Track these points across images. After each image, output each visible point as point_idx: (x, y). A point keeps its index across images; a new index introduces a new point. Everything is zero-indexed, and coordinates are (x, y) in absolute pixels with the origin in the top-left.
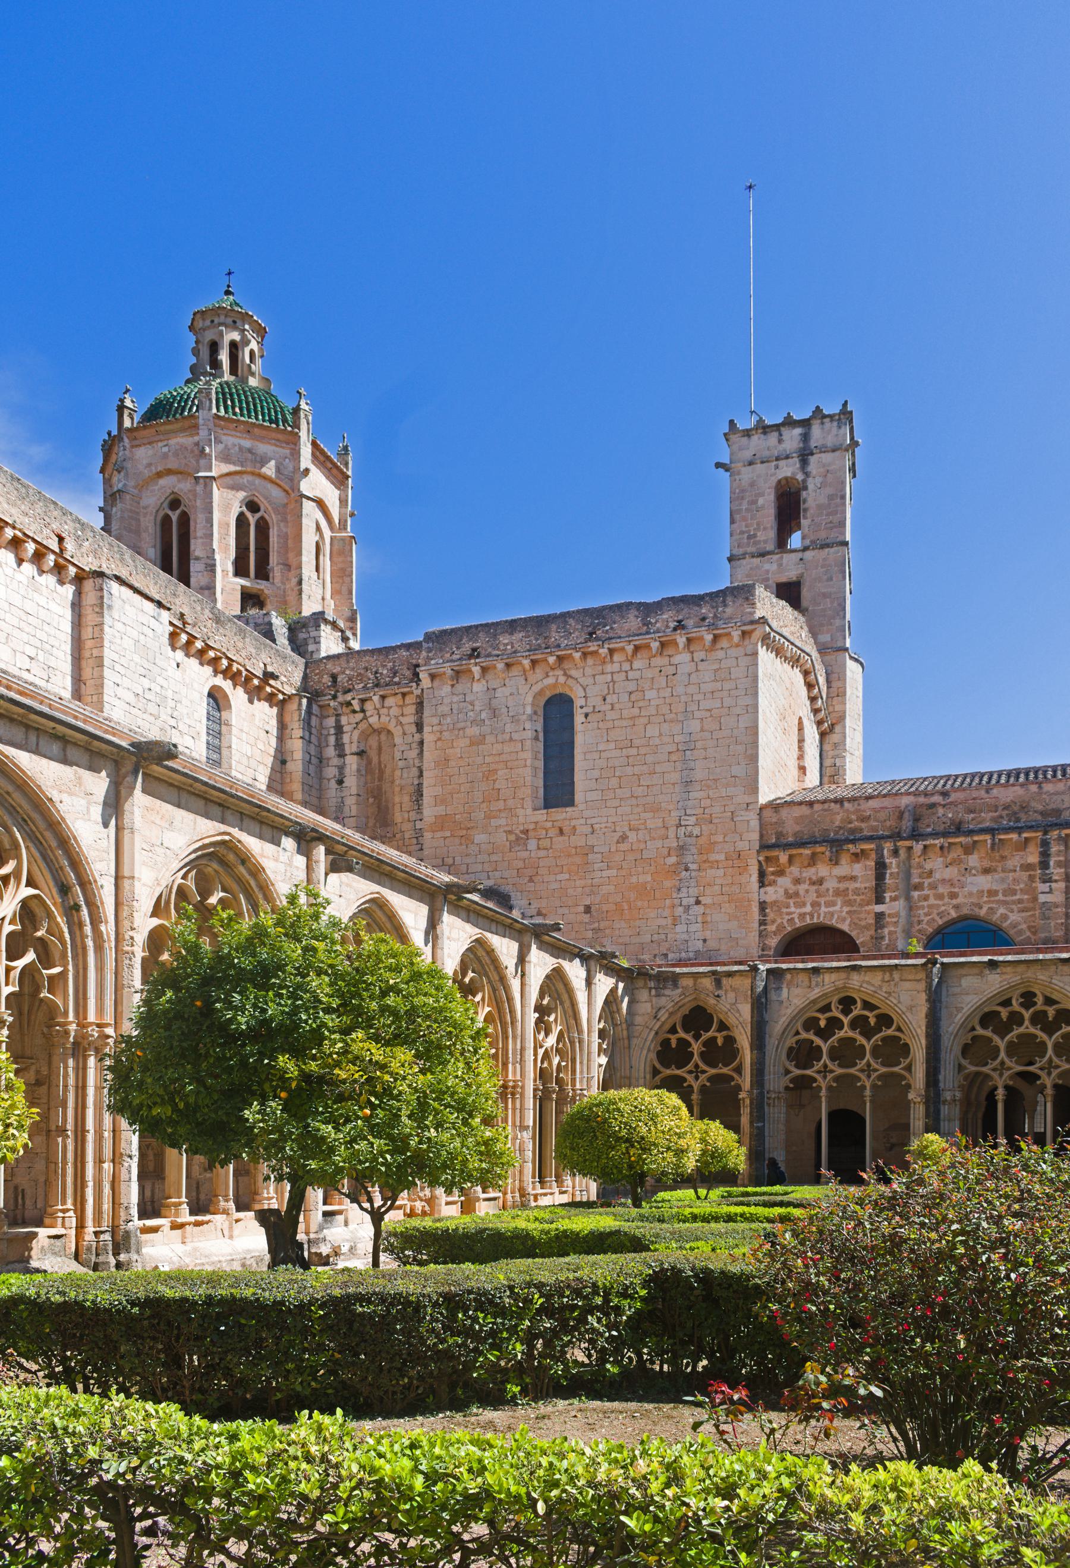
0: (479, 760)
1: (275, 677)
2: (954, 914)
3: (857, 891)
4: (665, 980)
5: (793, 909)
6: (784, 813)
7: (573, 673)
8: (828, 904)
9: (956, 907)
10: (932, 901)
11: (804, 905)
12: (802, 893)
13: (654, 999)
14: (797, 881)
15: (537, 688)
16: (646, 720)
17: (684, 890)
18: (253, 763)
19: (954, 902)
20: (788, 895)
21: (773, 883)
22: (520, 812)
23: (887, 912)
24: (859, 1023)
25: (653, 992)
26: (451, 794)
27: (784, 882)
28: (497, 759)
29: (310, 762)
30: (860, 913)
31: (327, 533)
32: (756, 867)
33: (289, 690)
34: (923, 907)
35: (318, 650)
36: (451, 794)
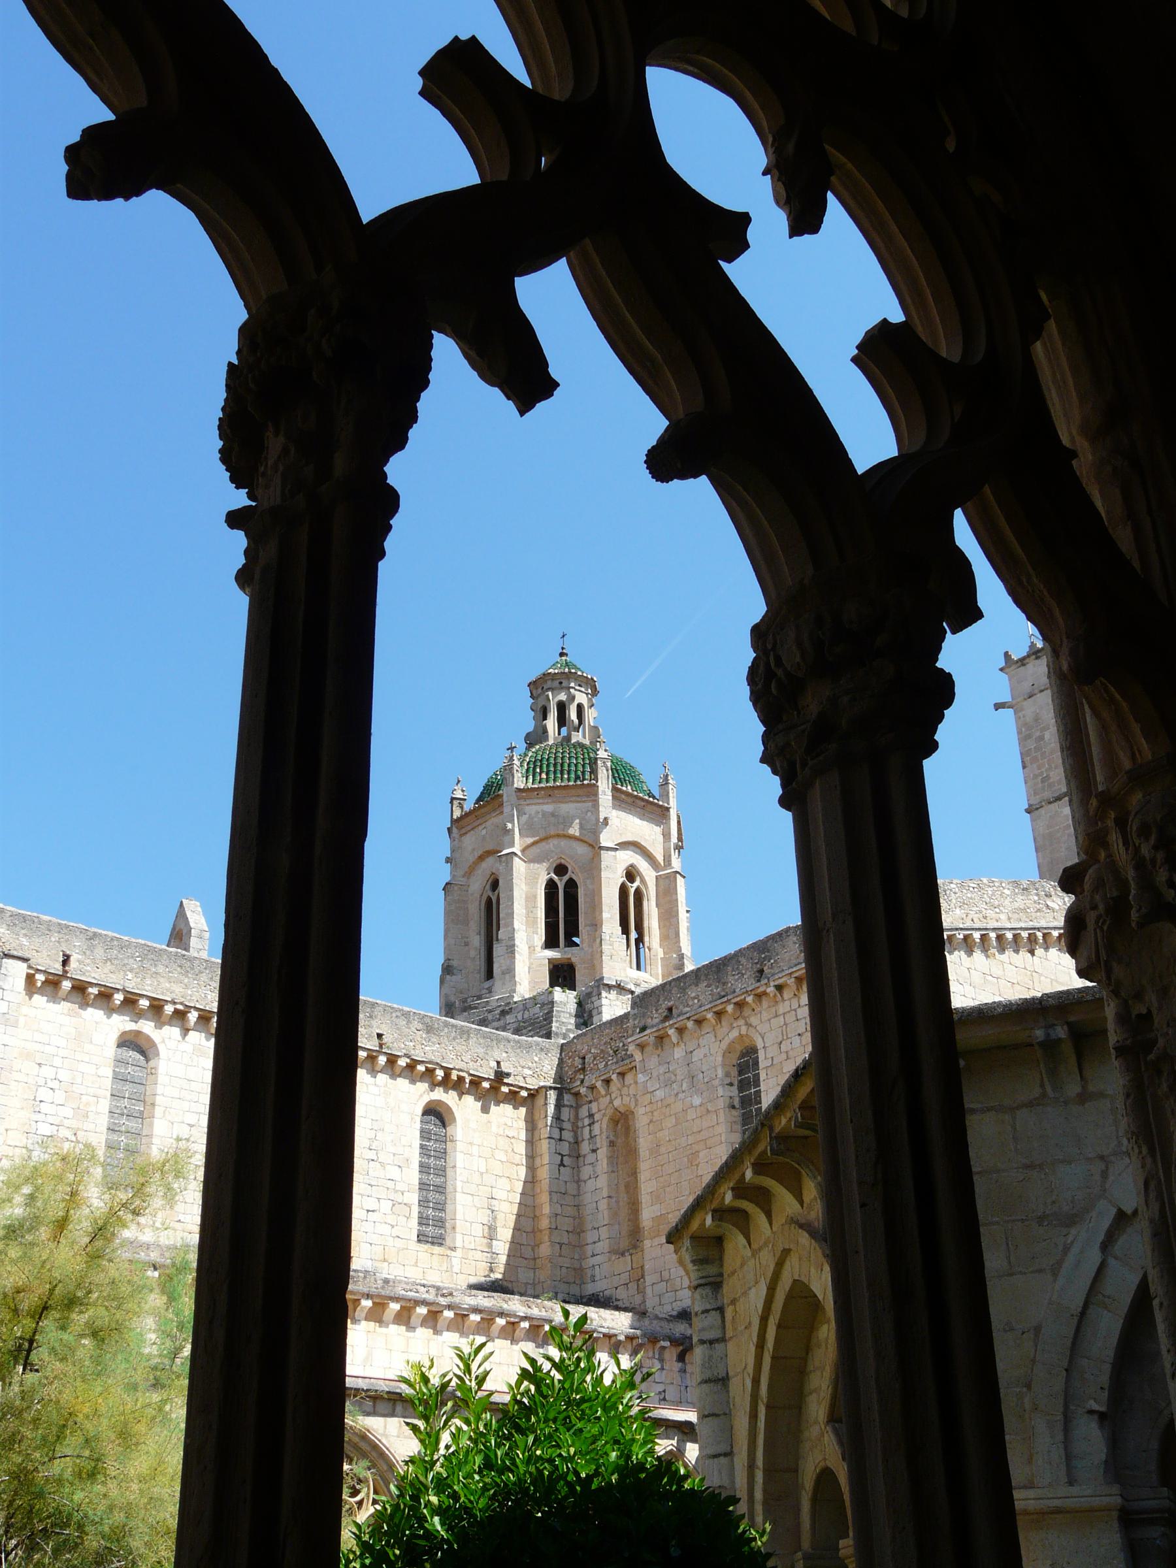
7: (754, 1020)
15: (724, 1045)
29: (562, 1164)
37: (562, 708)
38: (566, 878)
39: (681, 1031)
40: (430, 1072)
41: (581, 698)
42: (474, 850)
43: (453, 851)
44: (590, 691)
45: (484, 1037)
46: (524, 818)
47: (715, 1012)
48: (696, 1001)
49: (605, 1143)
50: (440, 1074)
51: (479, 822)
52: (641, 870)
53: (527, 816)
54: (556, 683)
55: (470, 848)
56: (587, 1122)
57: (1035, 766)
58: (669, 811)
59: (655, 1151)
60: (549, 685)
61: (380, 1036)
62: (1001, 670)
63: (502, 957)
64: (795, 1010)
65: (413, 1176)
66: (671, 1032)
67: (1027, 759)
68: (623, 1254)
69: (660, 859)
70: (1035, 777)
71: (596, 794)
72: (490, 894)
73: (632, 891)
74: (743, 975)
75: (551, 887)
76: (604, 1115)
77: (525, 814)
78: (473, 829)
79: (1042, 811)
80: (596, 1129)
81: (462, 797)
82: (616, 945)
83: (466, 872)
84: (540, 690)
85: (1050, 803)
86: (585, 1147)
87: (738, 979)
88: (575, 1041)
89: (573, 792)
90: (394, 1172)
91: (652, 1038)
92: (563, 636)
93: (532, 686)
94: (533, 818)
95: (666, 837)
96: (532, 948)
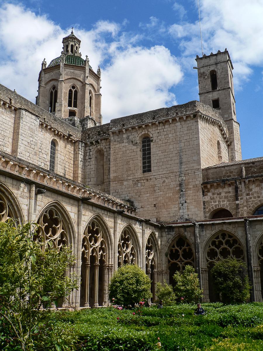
0: (125, 158)
1: (72, 136)
2: (259, 204)
3: (230, 197)
4: (170, 229)
5: (213, 203)
6: (210, 171)
7: (150, 130)
8: (223, 201)
9: (260, 201)
10: (253, 199)
11: (216, 202)
12: (215, 198)
13: (167, 235)
14: (213, 194)
15: (140, 135)
16: (169, 143)
17: (182, 198)
18: (65, 162)
19: (259, 199)
20: (211, 199)
21: (206, 195)
22: (136, 174)
23: (240, 203)
24: (227, 242)
25: (167, 232)
26: (118, 169)
27: (210, 194)
28: (130, 157)
30: (232, 204)
31: (94, 93)
32: (202, 190)
33: (76, 139)
34: (250, 201)
35: (87, 127)
36: (118, 169)
37: (72, 46)
39: (126, 130)
40: (54, 131)
42: (48, 78)
48: (132, 123)
49: (94, 157)
50: (57, 132)
51: (52, 71)
54: (71, 40)
56: (88, 151)
57: (202, 84)
59: (115, 160)
60: (70, 39)
61: (44, 119)
62: (196, 59)
64: (163, 129)
65: (49, 158)
66: (124, 130)
67: (200, 82)
68: (98, 185)
70: (202, 86)
71: (85, 69)
72: (52, 90)
74: (148, 118)
75: (70, 91)
76: (94, 150)
78: (48, 73)
79: (203, 95)
80: (91, 153)
82: (88, 109)
84: (66, 41)
85: (206, 93)
86: (87, 158)
87: (146, 119)
90: (45, 156)
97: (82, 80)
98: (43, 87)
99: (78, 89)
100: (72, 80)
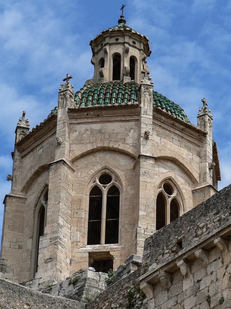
37: (117, 58)
38: (109, 185)
41: (133, 52)
42: (32, 167)
43: (14, 170)
44: (142, 48)
45: (6, 288)
46: (75, 134)
47: (222, 237)
51: (38, 142)
52: (179, 183)
53: (77, 133)
54: (113, 40)
55: (28, 167)
58: (206, 137)
60: (107, 40)
63: (46, 249)
69: (196, 175)
72: (43, 202)
73: (169, 201)
75: (96, 192)
77: (76, 131)
78: (32, 150)
81: (25, 126)
83: (24, 187)
88: (98, 300)
89: (119, 111)
91: (162, 273)
92: (123, 8)
93: (93, 44)
94: (82, 135)
95: (203, 158)
96: (75, 243)
97: (130, 150)
98: (14, 200)
99: (120, 181)
100: (99, 156)
